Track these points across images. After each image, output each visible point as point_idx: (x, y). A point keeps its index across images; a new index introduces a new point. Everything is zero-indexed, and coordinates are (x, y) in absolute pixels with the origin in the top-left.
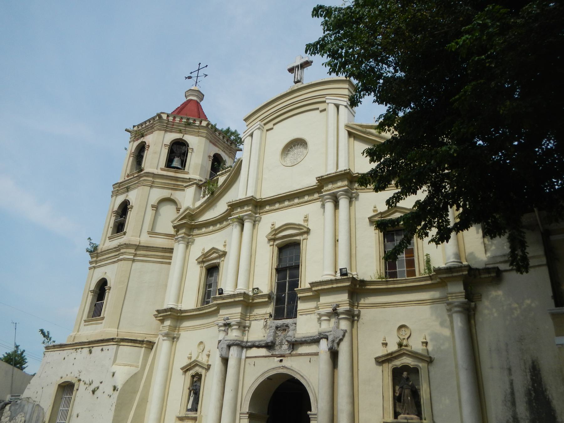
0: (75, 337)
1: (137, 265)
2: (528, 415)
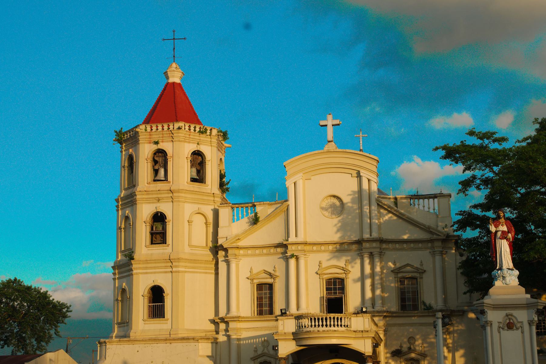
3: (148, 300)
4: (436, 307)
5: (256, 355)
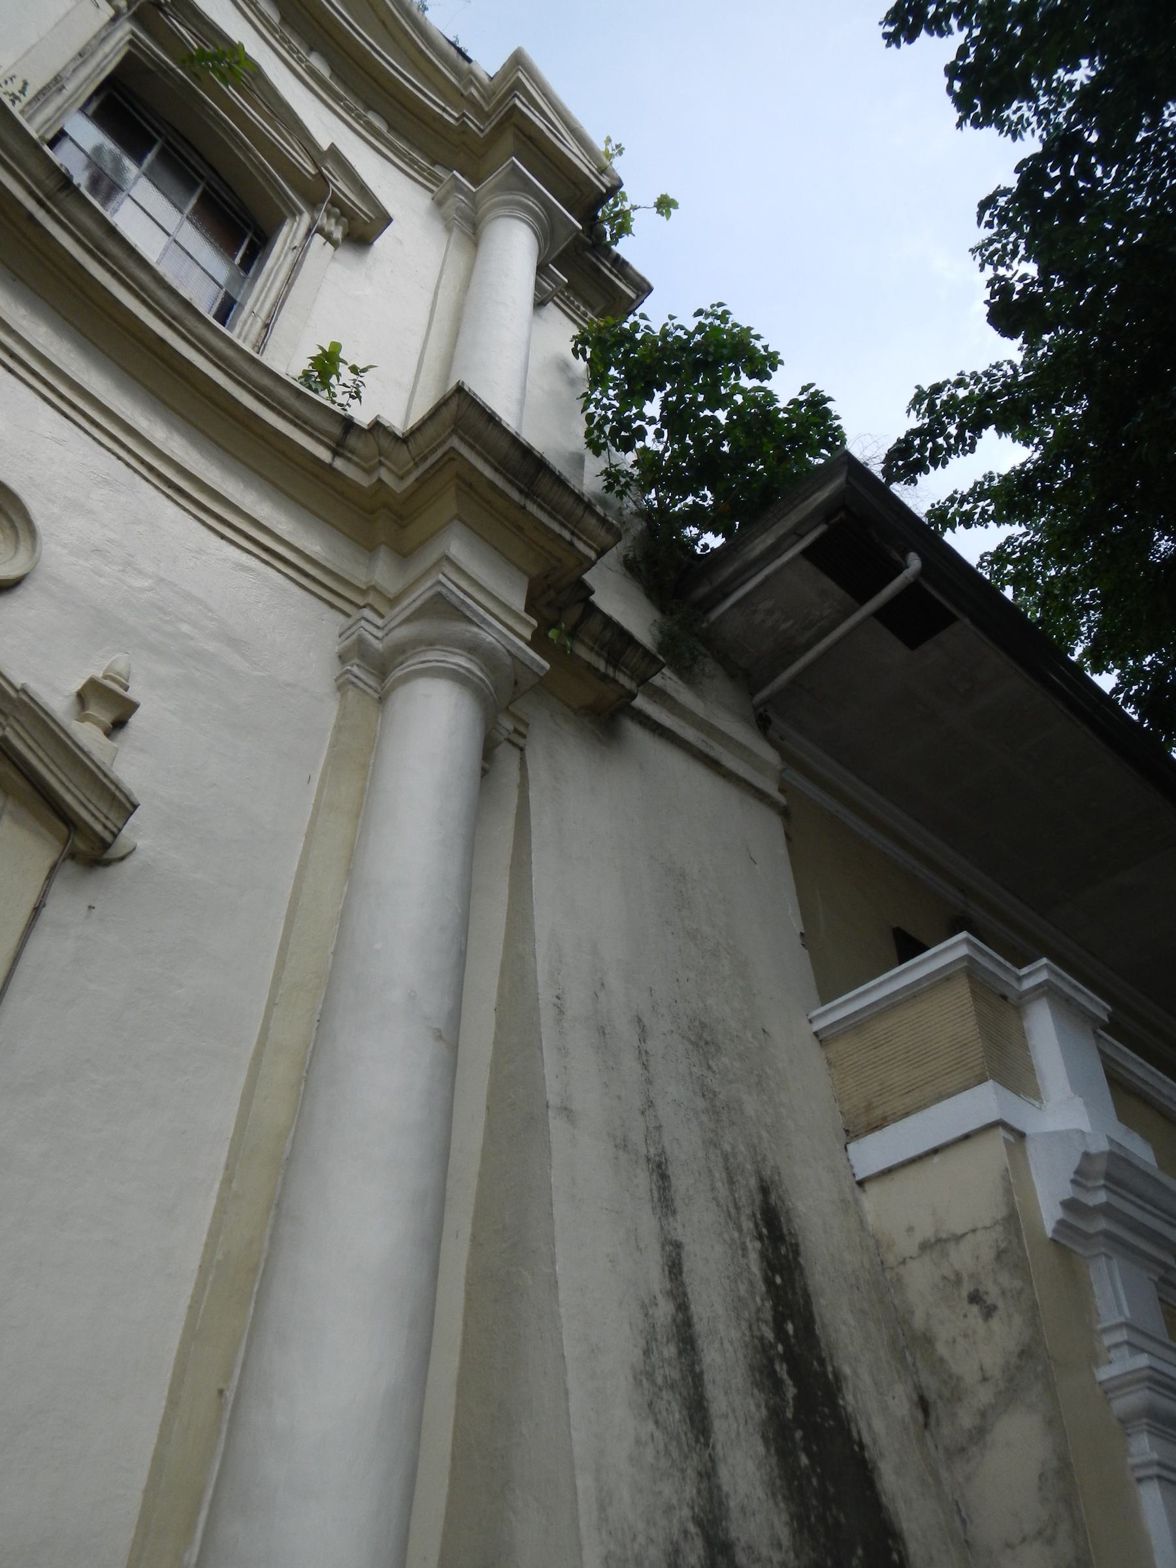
2: (784, 1534)
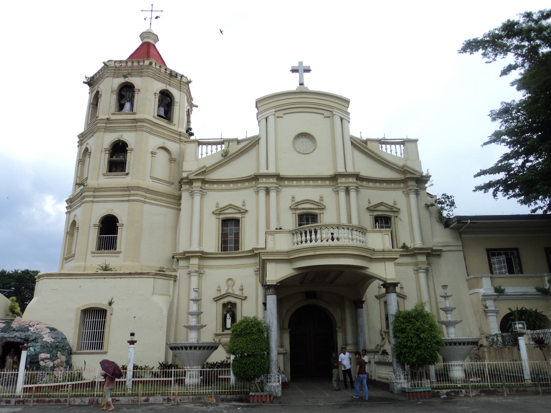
0: (85, 267)
1: (147, 207)
3: (99, 230)
4: (413, 246)
5: (219, 295)
